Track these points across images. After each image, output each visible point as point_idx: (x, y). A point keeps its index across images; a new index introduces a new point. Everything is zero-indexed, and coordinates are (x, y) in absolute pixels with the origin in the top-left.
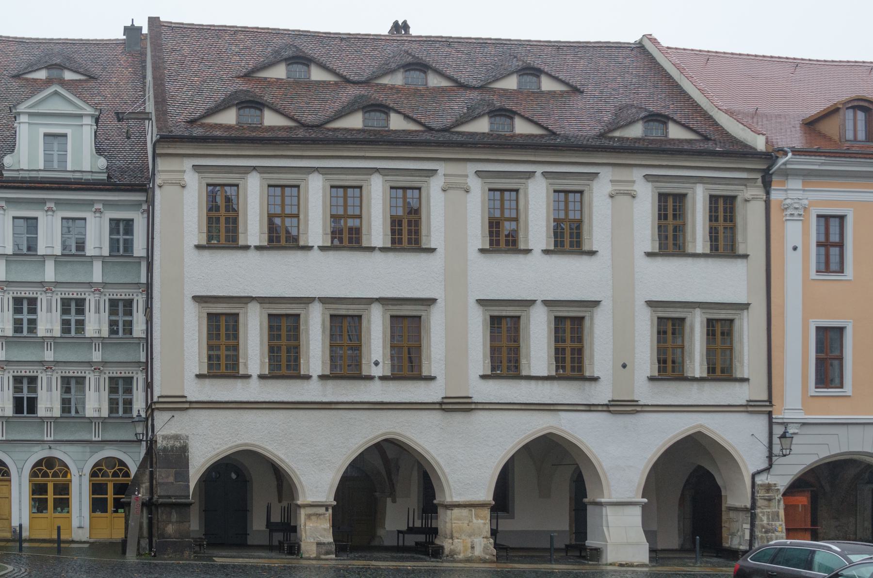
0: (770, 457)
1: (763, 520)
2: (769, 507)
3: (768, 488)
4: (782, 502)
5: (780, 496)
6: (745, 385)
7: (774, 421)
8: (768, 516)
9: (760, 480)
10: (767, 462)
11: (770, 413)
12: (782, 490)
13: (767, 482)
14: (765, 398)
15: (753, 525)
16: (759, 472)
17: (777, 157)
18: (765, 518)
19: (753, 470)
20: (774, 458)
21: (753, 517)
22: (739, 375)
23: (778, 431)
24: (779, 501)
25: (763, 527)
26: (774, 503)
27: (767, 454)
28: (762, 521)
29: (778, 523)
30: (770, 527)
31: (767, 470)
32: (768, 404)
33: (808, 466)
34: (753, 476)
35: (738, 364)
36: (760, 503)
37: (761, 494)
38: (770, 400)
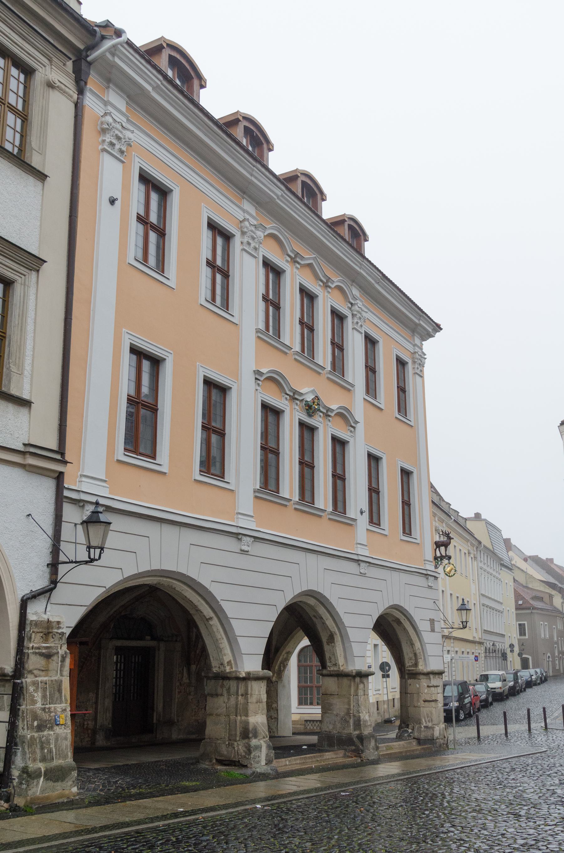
0: (54, 566)
1: (35, 701)
2: (46, 670)
3: (48, 630)
4: (68, 661)
5: (65, 647)
6: (24, 411)
7: (66, 493)
8: (45, 690)
9: (36, 612)
10: (47, 576)
11: (59, 477)
12: (68, 632)
13: (45, 617)
14: (54, 445)
15: (14, 711)
16: (35, 596)
17: (103, 38)
18: (38, 696)
19: (23, 590)
20: (62, 569)
21: (17, 694)
22: (14, 391)
23: (72, 515)
24: (63, 659)
25: (35, 717)
26: (55, 663)
27: (48, 559)
28: (34, 702)
29: (59, 707)
30: (45, 716)
31: (46, 592)
32: (58, 457)
33: (108, 590)
34: (24, 604)
35: (13, 368)
36: (33, 662)
37: (35, 642)
38: (61, 451)
